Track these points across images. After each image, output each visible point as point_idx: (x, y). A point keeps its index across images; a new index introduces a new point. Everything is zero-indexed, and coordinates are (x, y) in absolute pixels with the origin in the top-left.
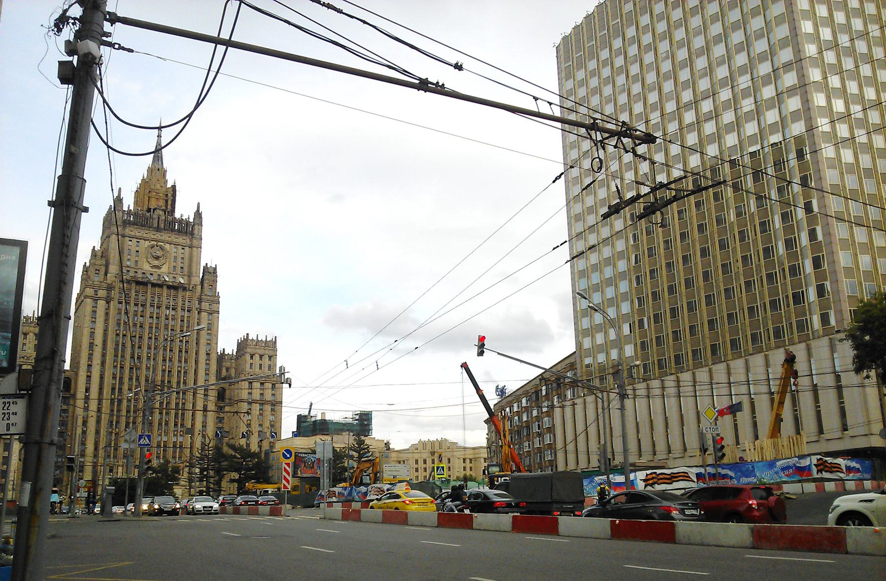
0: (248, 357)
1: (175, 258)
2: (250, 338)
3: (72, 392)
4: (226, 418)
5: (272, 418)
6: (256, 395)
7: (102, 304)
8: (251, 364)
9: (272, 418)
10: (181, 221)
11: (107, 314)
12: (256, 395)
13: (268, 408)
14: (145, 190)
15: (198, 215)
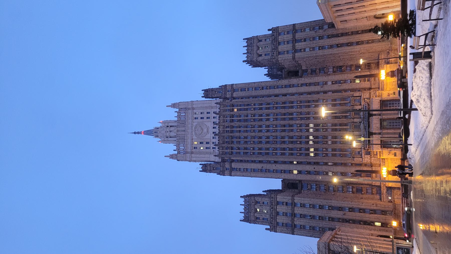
0: (260, 58)
1: (201, 118)
2: (246, 59)
3: (297, 182)
4: (311, 68)
5: (308, 30)
6: (289, 47)
7: (234, 165)
8: (265, 55)
9: (308, 30)
10: (179, 116)
11: (241, 161)
12: (289, 47)
13: (299, 35)
14: (166, 139)
15: (174, 106)
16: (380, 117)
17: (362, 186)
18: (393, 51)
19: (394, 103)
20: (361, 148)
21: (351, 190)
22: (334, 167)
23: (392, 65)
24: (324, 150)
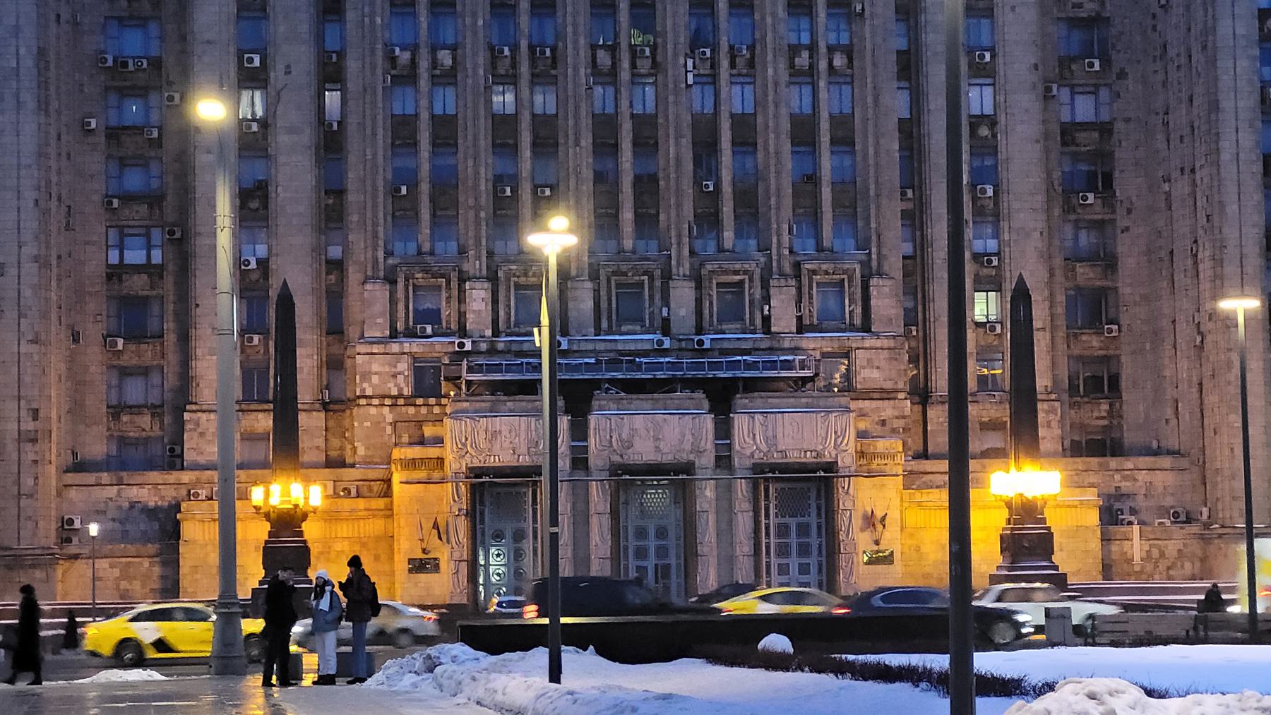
16: (707, 460)
17: (171, 338)
18: (1195, 547)
19: (813, 561)
20: (463, 332)
21: (135, 256)
22: (307, 136)
23: (1095, 544)
24: (445, 58)
